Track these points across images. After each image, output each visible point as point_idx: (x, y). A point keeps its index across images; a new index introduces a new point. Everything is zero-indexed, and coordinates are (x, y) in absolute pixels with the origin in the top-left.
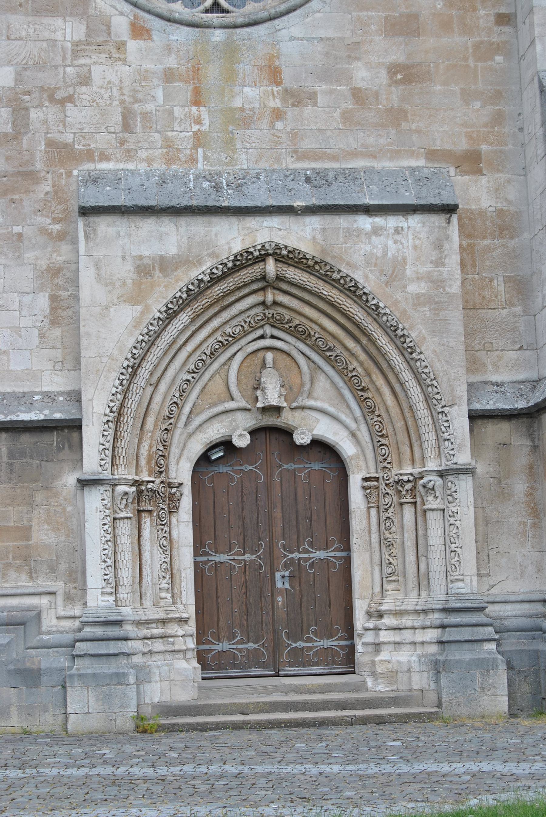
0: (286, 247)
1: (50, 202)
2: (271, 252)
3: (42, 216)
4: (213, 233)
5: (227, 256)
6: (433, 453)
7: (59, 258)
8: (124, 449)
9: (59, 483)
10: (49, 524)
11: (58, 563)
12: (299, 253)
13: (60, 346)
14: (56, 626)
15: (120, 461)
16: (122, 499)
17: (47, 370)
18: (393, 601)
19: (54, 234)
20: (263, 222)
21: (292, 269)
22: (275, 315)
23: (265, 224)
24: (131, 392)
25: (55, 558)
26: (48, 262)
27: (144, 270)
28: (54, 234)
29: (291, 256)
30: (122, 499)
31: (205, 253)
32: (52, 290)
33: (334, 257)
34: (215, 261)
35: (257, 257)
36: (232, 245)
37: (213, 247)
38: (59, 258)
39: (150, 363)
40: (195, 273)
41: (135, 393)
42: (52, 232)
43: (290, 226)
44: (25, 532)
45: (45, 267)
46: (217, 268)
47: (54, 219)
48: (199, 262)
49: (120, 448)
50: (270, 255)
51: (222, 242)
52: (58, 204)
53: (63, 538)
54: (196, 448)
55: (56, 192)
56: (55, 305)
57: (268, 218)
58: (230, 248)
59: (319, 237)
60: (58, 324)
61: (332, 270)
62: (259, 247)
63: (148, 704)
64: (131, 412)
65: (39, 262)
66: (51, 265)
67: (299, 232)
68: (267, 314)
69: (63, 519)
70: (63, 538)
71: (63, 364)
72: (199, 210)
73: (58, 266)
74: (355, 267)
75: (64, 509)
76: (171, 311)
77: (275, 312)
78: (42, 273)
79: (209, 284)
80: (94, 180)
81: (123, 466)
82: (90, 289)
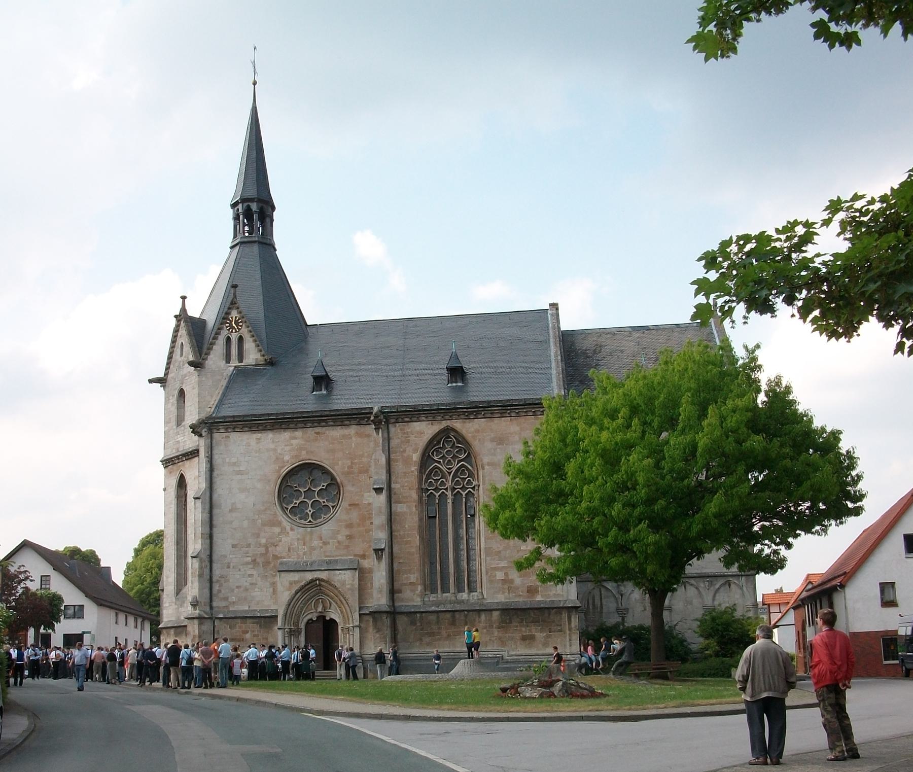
27: (291, 583)
44: (267, 639)
54: (305, 620)
80: (281, 563)
82: (280, 588)
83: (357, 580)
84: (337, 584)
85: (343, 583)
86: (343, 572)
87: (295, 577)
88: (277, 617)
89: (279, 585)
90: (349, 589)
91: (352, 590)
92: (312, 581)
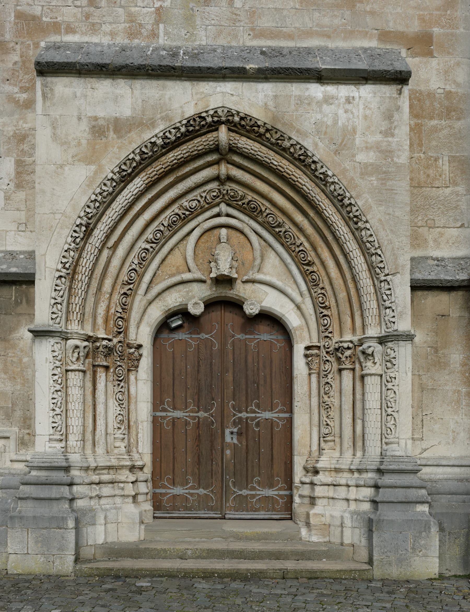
0: (238, 113)
1: (18, 71)
2: (224, 119)
3: (10, 84)
4: (167, 97)
5: (179, 120)
6: (374, 321)
7: (24, 125)
8: (78, 306)
9: (16, 335)
10: (5, 373)
11: (13, 411)
12: (251, 120)
13: (24, 209)
14: (9, 469)
15: (73, 317)
16: (73, 352)
17: (11, 231)
18: (328, 459)
19: (21, 102)
20: (216, 87)
21: (244, 139)
22: (229, 192)
23: (218, 89)
24: (86, 252)
25: (10, 405)
26: (14, 128)
28: (21, 102)
29: (243, 123)
30: (73, 352)
31: (159, 116)
32: (18, 156)
33: (284, 124)
34: (168, 124)
35: (210, 125)
36: (186, 109)
37: (167, 110)
38: (24, 125)
39: (105, 224)
40: (147, 135)
41: (89, 253)
42: (19, 100)
43: (242, 92)
45: (11, 133)
46: (170, 132)
47: (21, 88)
48: (153, 125)
49: (74, 305)
50: (223, 123)
51: (176, 105)
52: (26, 74)
53: (18, 387)
55: (24, 62)
56: (20, 169)
57: (222, 84)
58: (183, 112)
59: (271, 104)
60: (23, 187)
61: (282, 137)
62: (211, 112)
63: (91, 545)
64: (85, 271)
65: (6, 128)
66: (17, 132)
67: (252, 99)
68: (222, 190)
69: (19, 369)
70: (18, 387)
71: (26, 225)
72: (152, 70)
73: (24, 132)
74: (305, 135)
75: (21, 360)
76: (124, 173)
77: (229, 188)
78: (9, 138)
79: (164, 151)
80: (57, 47)
81: (77, 321)
82: (46, 149)
83: (403, 133)
84: (317, 148)
85: (343, 142)
86: (343, 91)
87: (121, 98)
88: (27, 281)
89: (43, 136)
90: (366, 171)
91: (382, 171)
92: (200, 126)
